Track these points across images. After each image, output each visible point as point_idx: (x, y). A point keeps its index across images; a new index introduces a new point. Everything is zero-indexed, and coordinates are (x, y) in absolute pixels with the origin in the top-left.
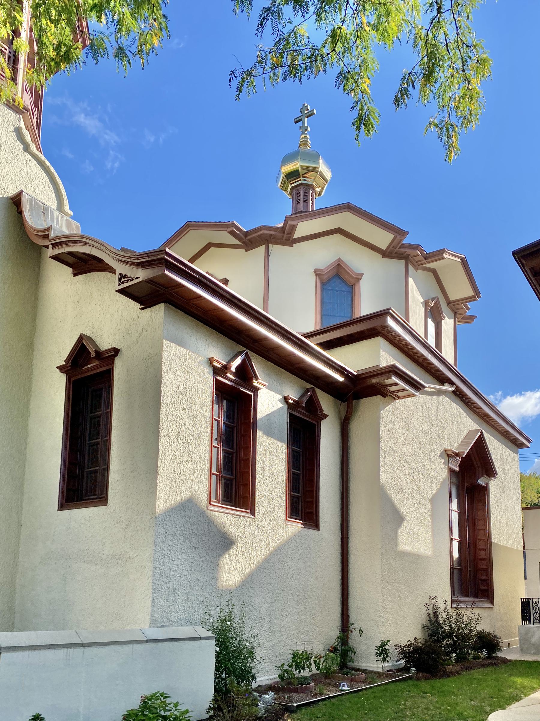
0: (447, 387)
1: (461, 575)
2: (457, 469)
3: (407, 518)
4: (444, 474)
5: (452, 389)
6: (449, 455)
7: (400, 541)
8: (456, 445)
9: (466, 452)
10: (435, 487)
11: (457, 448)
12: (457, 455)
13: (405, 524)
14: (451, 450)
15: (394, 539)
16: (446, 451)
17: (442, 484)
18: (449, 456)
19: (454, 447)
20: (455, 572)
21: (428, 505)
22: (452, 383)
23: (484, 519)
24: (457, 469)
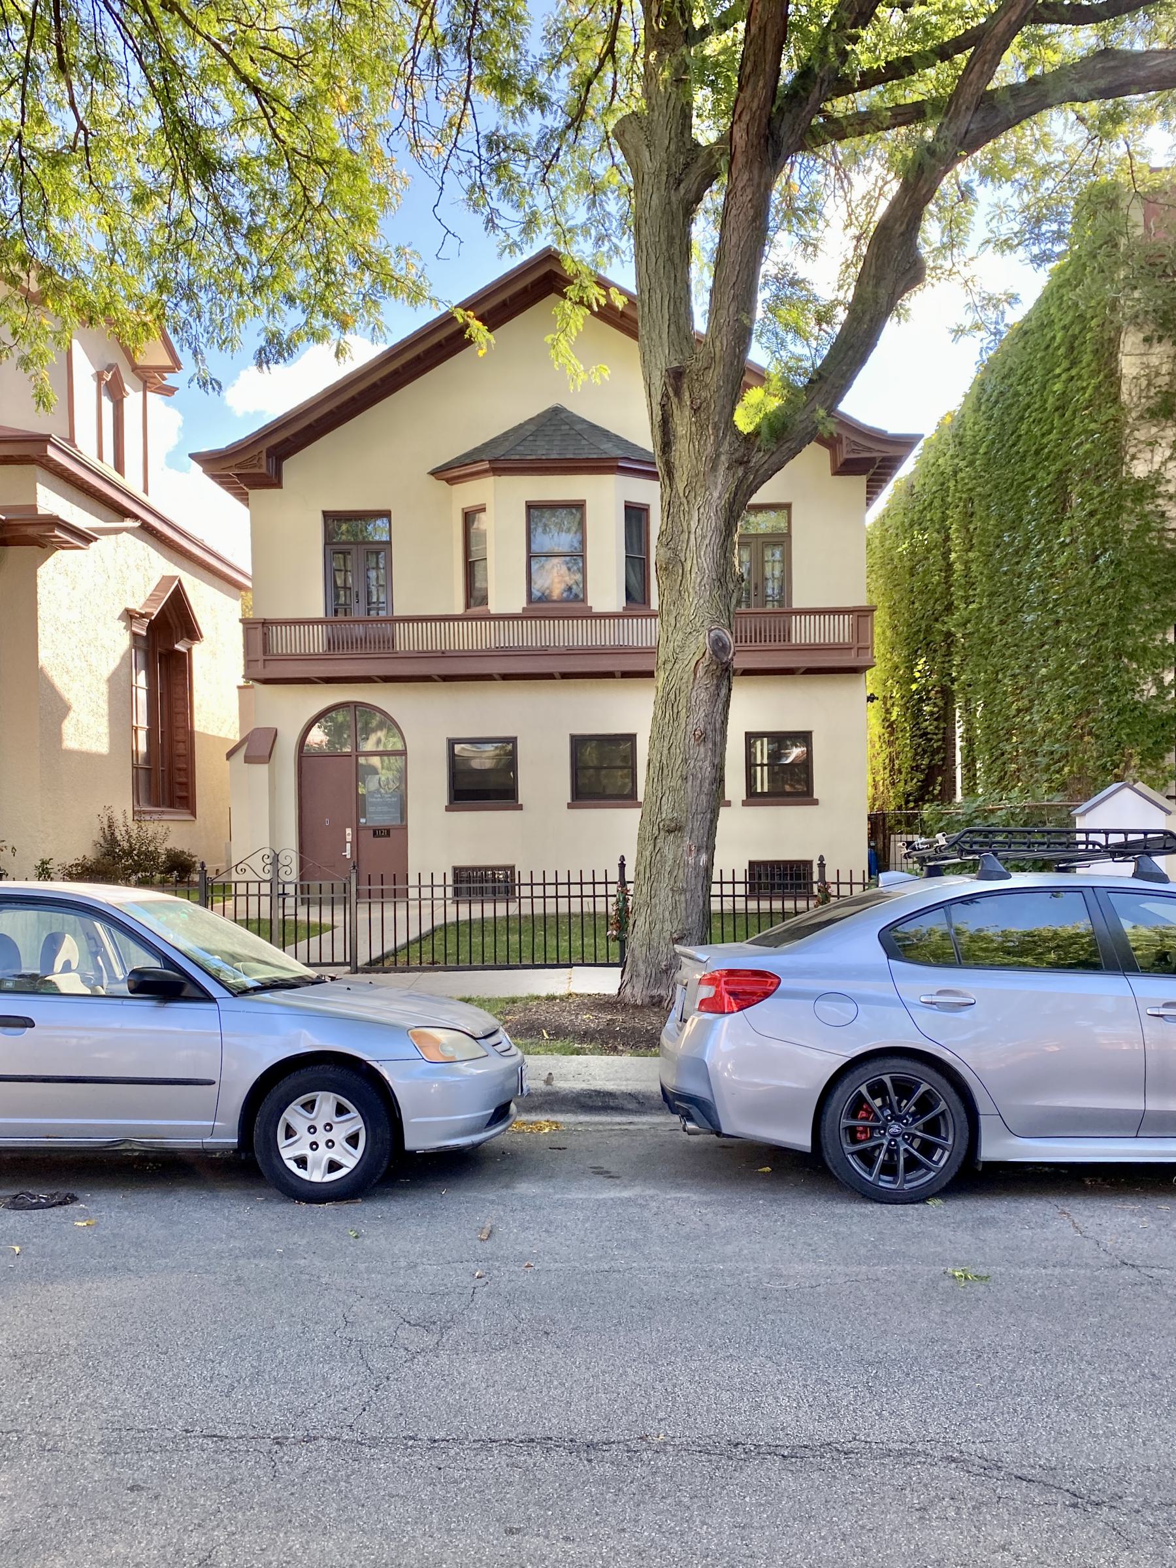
0: (129, 523)
1: (149, 782)
2: (144, 633)
3: (74, 707)
4: (125, 641)
5: (137, 524)
6: (130, 616)
7: (65, 737)
8: (142, 600)
9: (156, 613)
10: (114, 661)
11: (145, 605)
12: (142, 616)
13: (71, 714)
14: (134, 611)
15: (58, 736)
16: (127, 611)
17: (123, 658)
18: (132, 617)
19: (137, 604)
20: (142, 773)
21: (104, 688)
22: (136, 517)
23: (185, 699)
24: (144, 633)
